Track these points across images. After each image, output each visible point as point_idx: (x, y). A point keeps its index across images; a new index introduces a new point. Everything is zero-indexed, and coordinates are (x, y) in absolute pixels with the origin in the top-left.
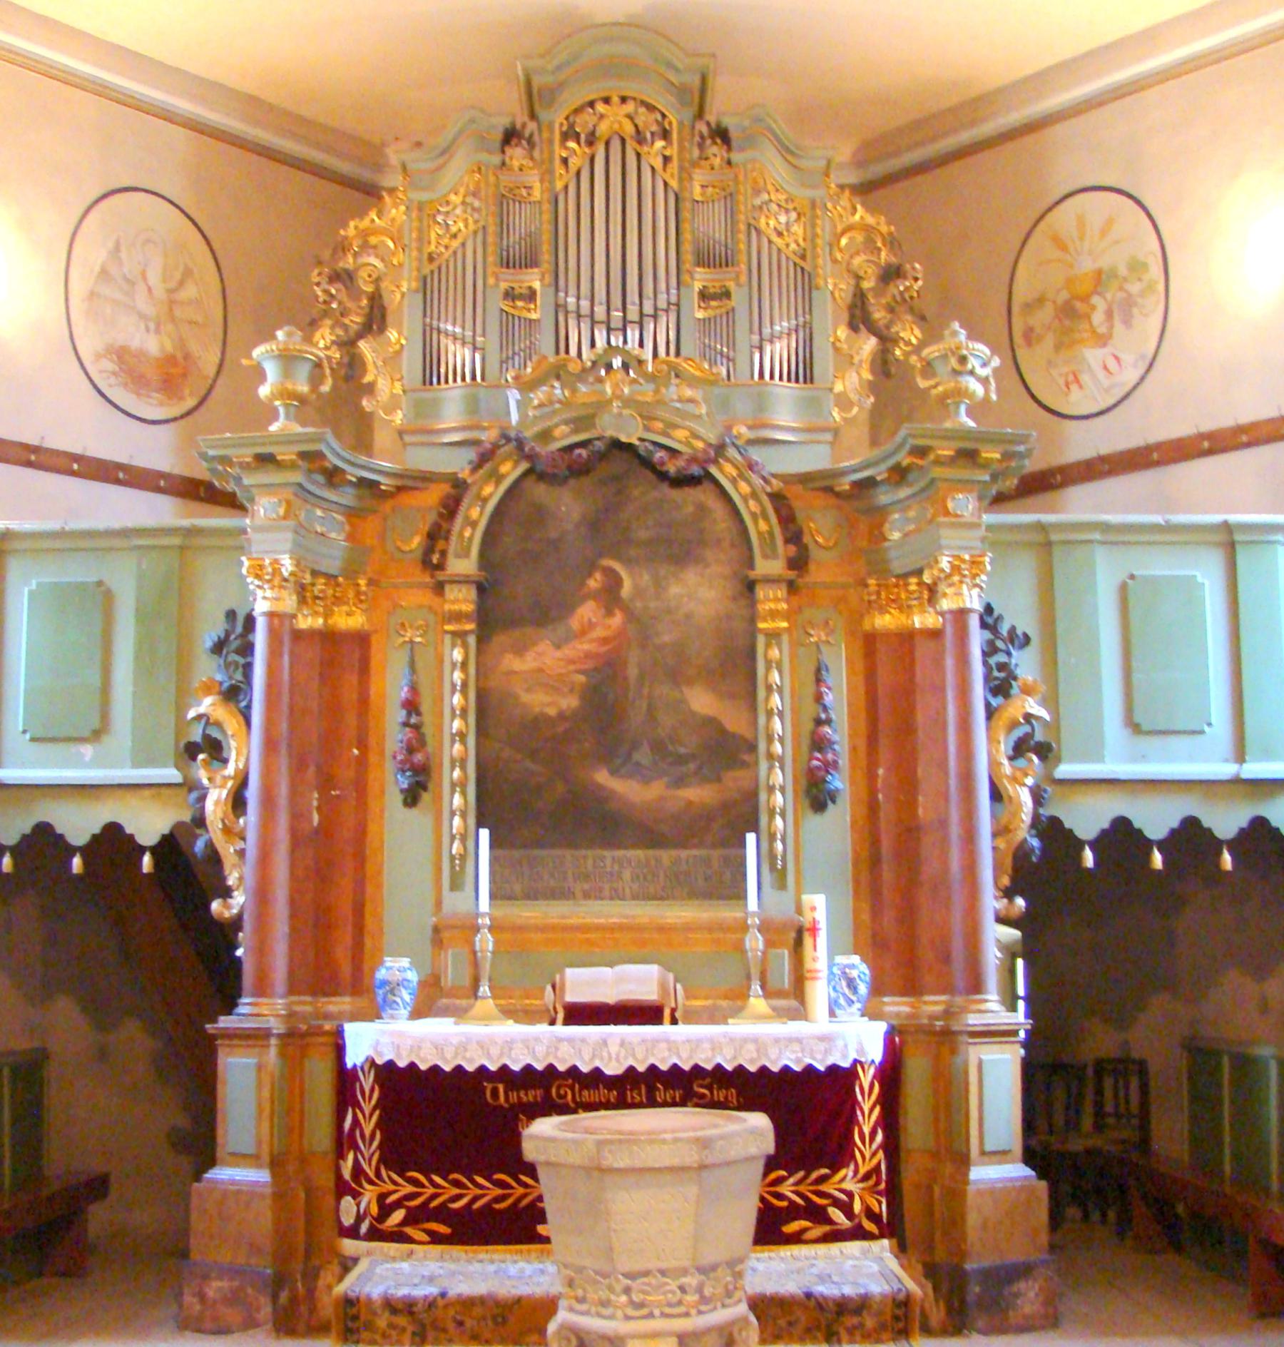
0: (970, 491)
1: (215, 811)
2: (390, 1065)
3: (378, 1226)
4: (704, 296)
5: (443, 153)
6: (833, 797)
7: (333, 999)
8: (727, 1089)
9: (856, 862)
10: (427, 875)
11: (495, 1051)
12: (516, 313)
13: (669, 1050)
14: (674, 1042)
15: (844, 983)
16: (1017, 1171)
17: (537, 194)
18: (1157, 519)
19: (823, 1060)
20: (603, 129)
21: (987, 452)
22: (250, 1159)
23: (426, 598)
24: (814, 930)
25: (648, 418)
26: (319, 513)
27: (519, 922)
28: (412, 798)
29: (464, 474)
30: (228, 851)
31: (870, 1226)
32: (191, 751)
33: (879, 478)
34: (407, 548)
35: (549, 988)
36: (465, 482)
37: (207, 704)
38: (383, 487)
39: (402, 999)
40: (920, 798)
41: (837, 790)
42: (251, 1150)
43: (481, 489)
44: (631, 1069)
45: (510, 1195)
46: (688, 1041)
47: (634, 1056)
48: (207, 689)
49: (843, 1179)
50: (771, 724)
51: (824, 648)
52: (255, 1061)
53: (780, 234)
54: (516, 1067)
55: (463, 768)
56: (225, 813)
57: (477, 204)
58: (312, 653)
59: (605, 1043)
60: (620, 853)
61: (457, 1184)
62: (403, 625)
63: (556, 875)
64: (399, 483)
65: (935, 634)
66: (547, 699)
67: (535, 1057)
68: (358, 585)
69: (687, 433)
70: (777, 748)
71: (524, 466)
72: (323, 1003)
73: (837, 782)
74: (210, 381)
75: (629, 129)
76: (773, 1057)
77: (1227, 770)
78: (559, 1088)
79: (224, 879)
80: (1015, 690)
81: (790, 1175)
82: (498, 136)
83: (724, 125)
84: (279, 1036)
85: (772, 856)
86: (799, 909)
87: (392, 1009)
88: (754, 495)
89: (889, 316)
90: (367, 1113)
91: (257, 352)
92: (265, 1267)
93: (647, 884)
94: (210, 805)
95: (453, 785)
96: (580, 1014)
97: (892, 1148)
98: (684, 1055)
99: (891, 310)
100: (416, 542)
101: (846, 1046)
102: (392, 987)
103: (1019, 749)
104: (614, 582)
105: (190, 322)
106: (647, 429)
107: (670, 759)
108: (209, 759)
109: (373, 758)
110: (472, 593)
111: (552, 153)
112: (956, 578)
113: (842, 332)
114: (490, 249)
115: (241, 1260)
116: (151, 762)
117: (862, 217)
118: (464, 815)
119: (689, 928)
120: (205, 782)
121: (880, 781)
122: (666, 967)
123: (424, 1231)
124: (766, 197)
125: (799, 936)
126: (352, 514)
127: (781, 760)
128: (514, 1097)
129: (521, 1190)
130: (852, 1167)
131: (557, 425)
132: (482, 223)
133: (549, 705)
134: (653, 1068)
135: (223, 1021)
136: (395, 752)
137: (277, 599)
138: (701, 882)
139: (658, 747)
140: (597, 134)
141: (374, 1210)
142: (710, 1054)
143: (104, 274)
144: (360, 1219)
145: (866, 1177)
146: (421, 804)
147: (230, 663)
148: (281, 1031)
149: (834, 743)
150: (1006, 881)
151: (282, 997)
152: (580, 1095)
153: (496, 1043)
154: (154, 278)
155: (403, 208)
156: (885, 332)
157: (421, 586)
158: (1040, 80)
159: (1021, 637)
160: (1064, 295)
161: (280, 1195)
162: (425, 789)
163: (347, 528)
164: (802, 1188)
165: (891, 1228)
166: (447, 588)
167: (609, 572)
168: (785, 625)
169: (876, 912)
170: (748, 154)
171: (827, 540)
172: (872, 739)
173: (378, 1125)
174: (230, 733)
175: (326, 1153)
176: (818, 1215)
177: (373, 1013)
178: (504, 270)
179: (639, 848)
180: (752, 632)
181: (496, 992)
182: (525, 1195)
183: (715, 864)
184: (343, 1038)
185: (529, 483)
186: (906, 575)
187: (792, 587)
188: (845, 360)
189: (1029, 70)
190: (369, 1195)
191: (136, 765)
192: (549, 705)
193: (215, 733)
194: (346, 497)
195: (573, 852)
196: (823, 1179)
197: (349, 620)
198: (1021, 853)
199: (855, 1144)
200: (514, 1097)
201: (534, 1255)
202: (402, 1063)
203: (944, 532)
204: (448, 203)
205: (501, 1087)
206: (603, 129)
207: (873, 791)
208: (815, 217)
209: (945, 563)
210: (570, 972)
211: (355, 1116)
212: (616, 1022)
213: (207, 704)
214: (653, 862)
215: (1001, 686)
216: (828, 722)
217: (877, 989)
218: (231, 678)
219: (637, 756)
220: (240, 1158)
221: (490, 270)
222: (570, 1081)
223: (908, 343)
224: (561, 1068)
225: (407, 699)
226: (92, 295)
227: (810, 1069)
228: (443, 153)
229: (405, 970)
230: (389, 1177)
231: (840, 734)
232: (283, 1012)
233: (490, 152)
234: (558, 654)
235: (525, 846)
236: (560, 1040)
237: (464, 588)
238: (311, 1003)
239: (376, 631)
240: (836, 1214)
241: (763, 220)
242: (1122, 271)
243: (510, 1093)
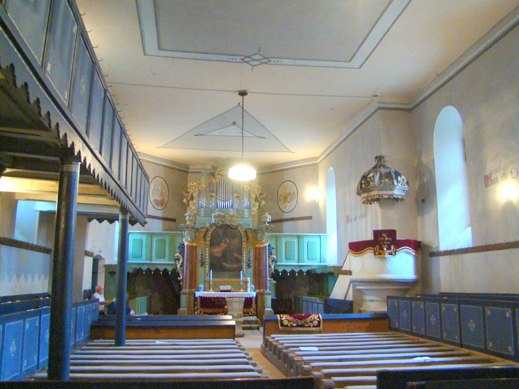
4: (236, 197)
16: (270, 309)
17: (214, 183)
18: (290, 234)
24: (248, 282)
25: (230, 221)
28: (202, 266)
29: (209, 228)
30: (180, 272)
31: (254, 315)
32: (176, 260)
48: (178, 252)
54: (215, 297)
65: (263, 248)
73: (251, 265)
77: (297, 264)
80: (272, 254)
85: (244, 273)
86: (247, 279)
88: (242, 231)
91: (186, 214)
94: (178, 266)
96: (222, 291)
97: (257, 307)
100: (203, 235)
102: (201, 288)
103: (273, 261)
109: (197, 261)
110: (209, 242)
113: (254, 202)
125: (246, 282)
126: (195, 232)
143: (154, 189)
150: (271, 276)
160: (285, 195)
165: (256, 315)
169: (256, 280)
172: (255, 260)
176: (248, 313)
177: (198, 291)
180: (242, 247)
181: (212, 289)
187: (247, 242)
188: (254, 206)
189: (281, 163)
190: (199, 311)
193: (178, 258)
197: (194, 244)
198: (272, 273)
209: (264, 240)
210: (220, 286)
215: (270, 254)
217: (255, 289)
226: (152, 193)
231: (252, 259)
242: (292, 193)
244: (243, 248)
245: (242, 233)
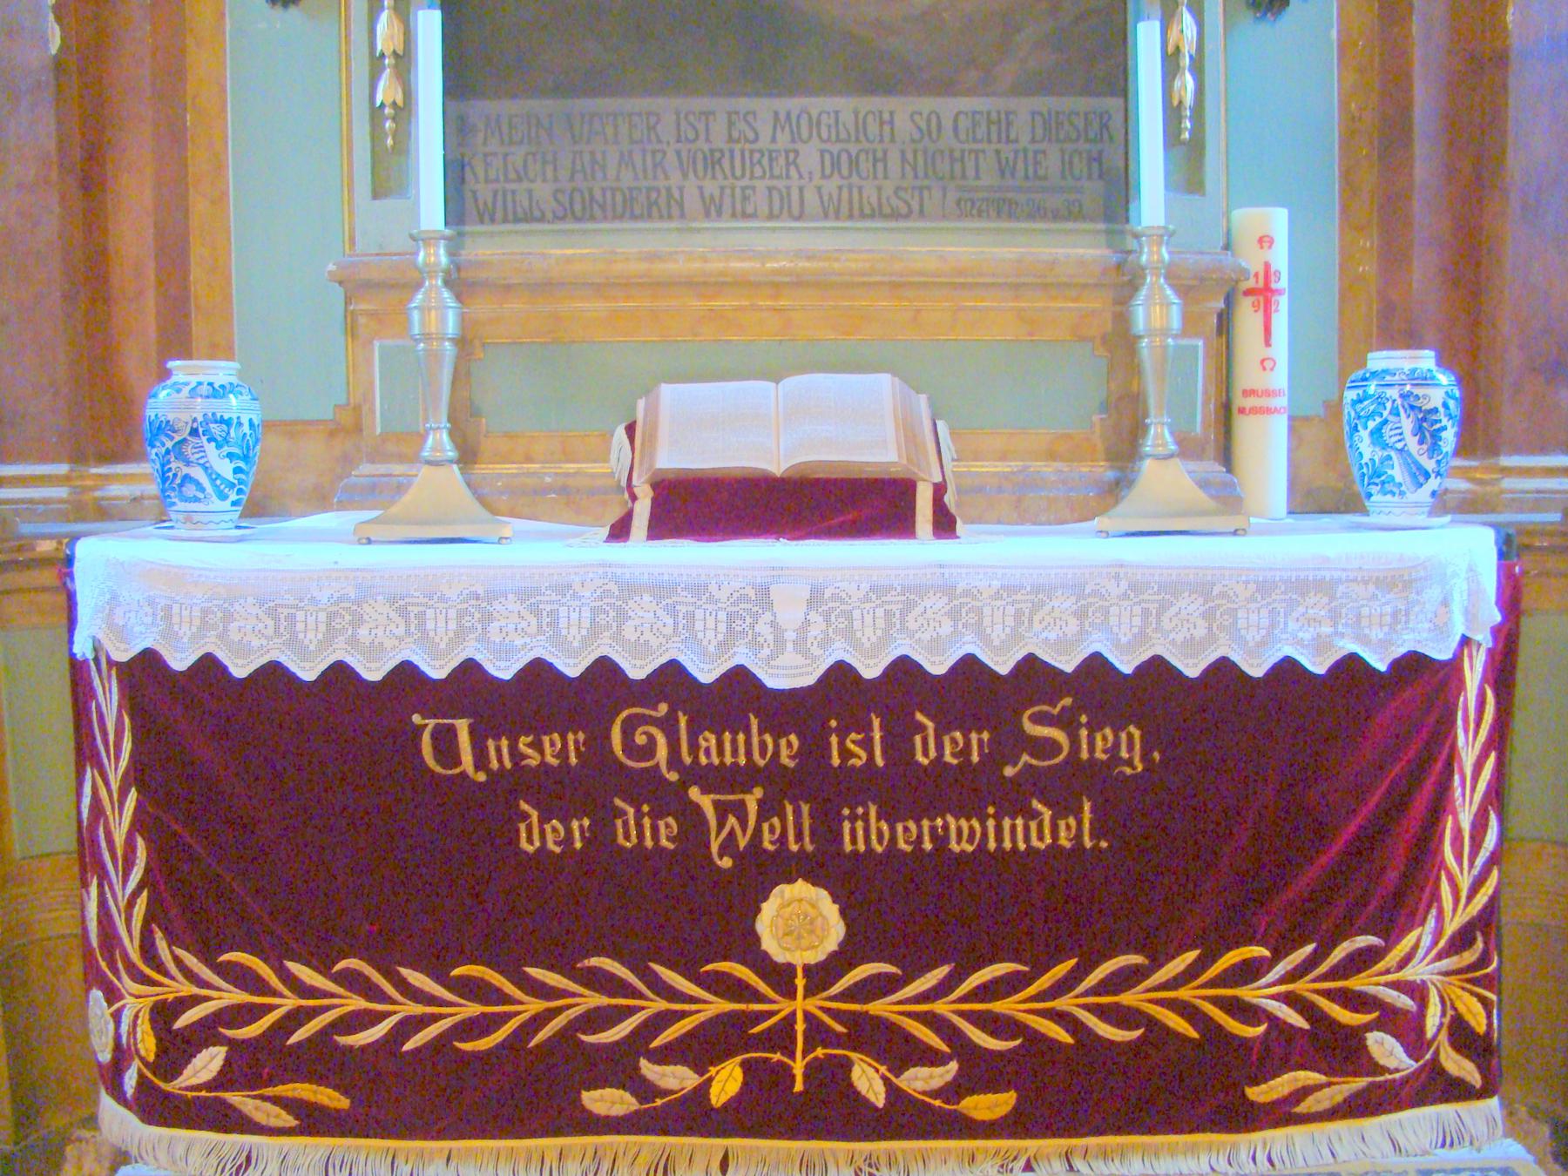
2: (149, 660)
3: (167, 1087)
7: (119, 469)
9: (1346, 142)
11: (441, 627)
13: (954, 615)
15: (1407, 424)
19: (1385, 644)
44: (841, 673)
45: (506, 1017)
46: (1011, 589)
47: (848, 634)
59: (764, 596)
60: (794, 104)
63: (638, 159)
67: (558, 640)
76: (1252, 636)
78: (628, 732)
81: (1278, 955)
93: (855, 179)
98: (998, 634)
101: (1445, 603)
119: (961, 283)
122: (911, 380)
123: (275, 1100)
129: (535, 1006)
130: (1431, 922)
134: (904, 669)
138: (989, 179)
141: (147, 1044)
144: (122, 1054)
145: (1462, 940)
152: (694, 747)
164: (1302, 986)
169: (1393, 257)
173: (138, 825)
179: (840, 93)
183: (1022, 130)
195: (677, 102)
196: (1361, 961)
199: (1443, 862)
200: (499, 752)
202: (179, 661)
205: (462, 726)
210: (667, 391)
214: (873, 129)
222: (663, 708)
224: (637, 669)
229: (218, 392)
230: (178, 961)
235: (558, 91)
236: (630, 589)
240: (1386, 1049)
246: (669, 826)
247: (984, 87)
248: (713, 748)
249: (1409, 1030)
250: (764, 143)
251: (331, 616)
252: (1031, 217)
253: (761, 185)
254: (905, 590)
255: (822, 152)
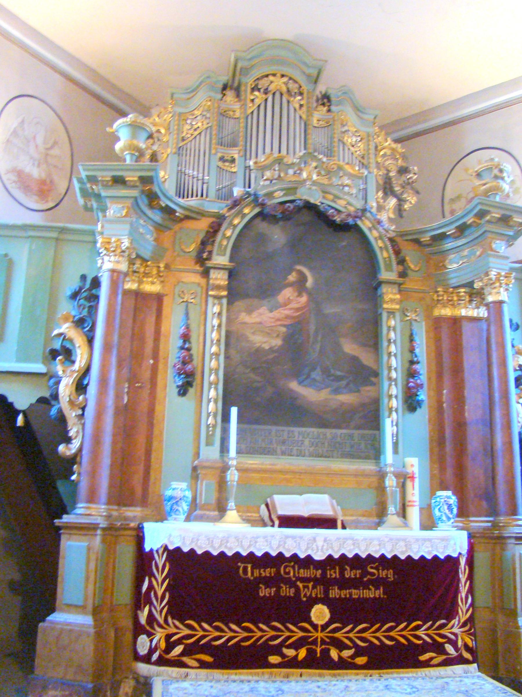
0: (503, 240)
1: (65, 391)
2: (178, 550)
5: (193, 91)
6: (419, 404)
8: (388, 570)
10: (190, 436)
11: (246, 543)
12: (225, 168)
13: (354, 544)
14: (356, 540)
15: (446, 507)
19: (443, 553)
20: (272, 87)
21: (516, 218)
22: (81, 609)
23: (197, 279)
24: (412, 478)
26: (142, 222)
27: (247, 466)
28: (183, 391)
30: (71, 415)
31: (467, 655)
32: (54, 354)
33: (469, 222)
34: (188, 250)
35: (263, 507)
36: (224, 216)
37: (66, 328)
38: (177, 214)
39: (183, 508)
40: (466, 407)
41: (422, 401)
42: (81, 603)
43: (233, 219)
44: (330, 557)
45: (253, 637)
47: (332, 548)
48: (66, 319)
49: (453, 627)
50: (390, 361)
51: (414, 323)
52: (87, 544)
53: (353, 146)
55: (217, 375)
56: (71, 392)
57: (208, 115)
58: (130, 303)
59: (314, 540)
60: (304, 429)
61: (218, 629)
62: (183, 292)
64: (187, 213)
66: (265, 340)
67: (271, 547)
68: (159, 267)
69: (345, 203)
70: (394, 375)
71: (257, 210)
72: (124, 510)
73: (422, 396)
74: (62, 197)
75: (284, 89)
79: (67, 432)
81: (424, 624)
82: (220, 86)
83: (328, 94)
84: (104, 529)
87: (176, 514)
88: (380, 237)
89: (402, 190)
90: (160, 580)
92: (87, 682)
95: (211, 384)
98: (363, 548)
99: (403, 187)
102: (177, 501)
104: (303, 279)
105: (55, 166)
106: (324, 197)
107: (332, 378)
108: (63, 360)
109: (161, 366)
110: (226, 276)
111: (246, 97)
112: (497, 284)
114: (214, 137)
115: (70, 676)
116: (27, 360)
117: (389, 144)
118: (216, 401)
120: (60, 373)
121: (444, 397)
122: (332, 497)
123: (195, 659)
124: (346, 128)
126: (159, 228)
127: (395, 380)
128: (256, 573)
129: (259, 634)
130: (457, 618)
131: (276, 191)
132: (210, 125)
133: (265, 343)
134: (343, 556)
135: (66, 518)
136: (175, 364)
137: (118, 262)
139: (326, 372)
140: (269, 89)
141: (163, 645)
142: (378, 548)
144: (151, 651)
145: (464, 625)
146: (188, 395)
147: (81, 305)
148: (105, 526)
149: (421, 375)
151: (105, 504)
152: (298, 573)
153: (247, 538)
154: (40, 140)
155: (170, 115)
156: (400, 196)
157: (195, 272)
158: (459, 102)
159: (515, 324)
161: (99, 635)
162: (191, 386)
163: (155, 235)
166: (212, 271)
167: (300, 273)
168: (397, 307)
170: (339, 108)
171: (415, 267)
172: (440, 375)
174: (77, 345)
175: (126, 605)
176: (439, 649)
178: (220, 147)
182: (261, 637)
184: (143, 532)
185: (258, 220)
186: (455, 288)
189: (454, 98)
190: (159, 635)
191: (19, 360)
192: (265, 343)
193: (68, 345)
194: (157, 216)
199: (459, 605)
201: (267, 676)
202: (186, 549)
203: (491, 259)
204: (193, 115)
205: (249, 567)
206: (272, 87)
207: (440, 403)
208: (369, 141)
211: (150, 582)
212: (313, 527)
213: (66, 328)
216: (418, 362)
218: (81, 313)
219: (313, 375)
220: (72, 607)
221: (213, 146)
222: (292, 564)
223: (411, 203)
224: (287, 555)
225: (183, 333)
227: (436, 557)
228: (193, 91)
230: (173, 623)
232: (104, 514)
233: (216, 93)
234: (271, 315)
236: (287, 537)
237: (222, 272)
238: (117, 510)
239: (167, 295)
240: (449, 648)
241: (346, 138)
243: (255, 570)
244: (385, 315)
245: (377, 245)
246: (293, 590)
247: (347, 428)
248: (303, 573)
249: (454, 644)
250: (296, 438)
251: (221, 541)
252: (358, 458)
253: (295, 448)
254: (344, 539)
255: (310, 441)
